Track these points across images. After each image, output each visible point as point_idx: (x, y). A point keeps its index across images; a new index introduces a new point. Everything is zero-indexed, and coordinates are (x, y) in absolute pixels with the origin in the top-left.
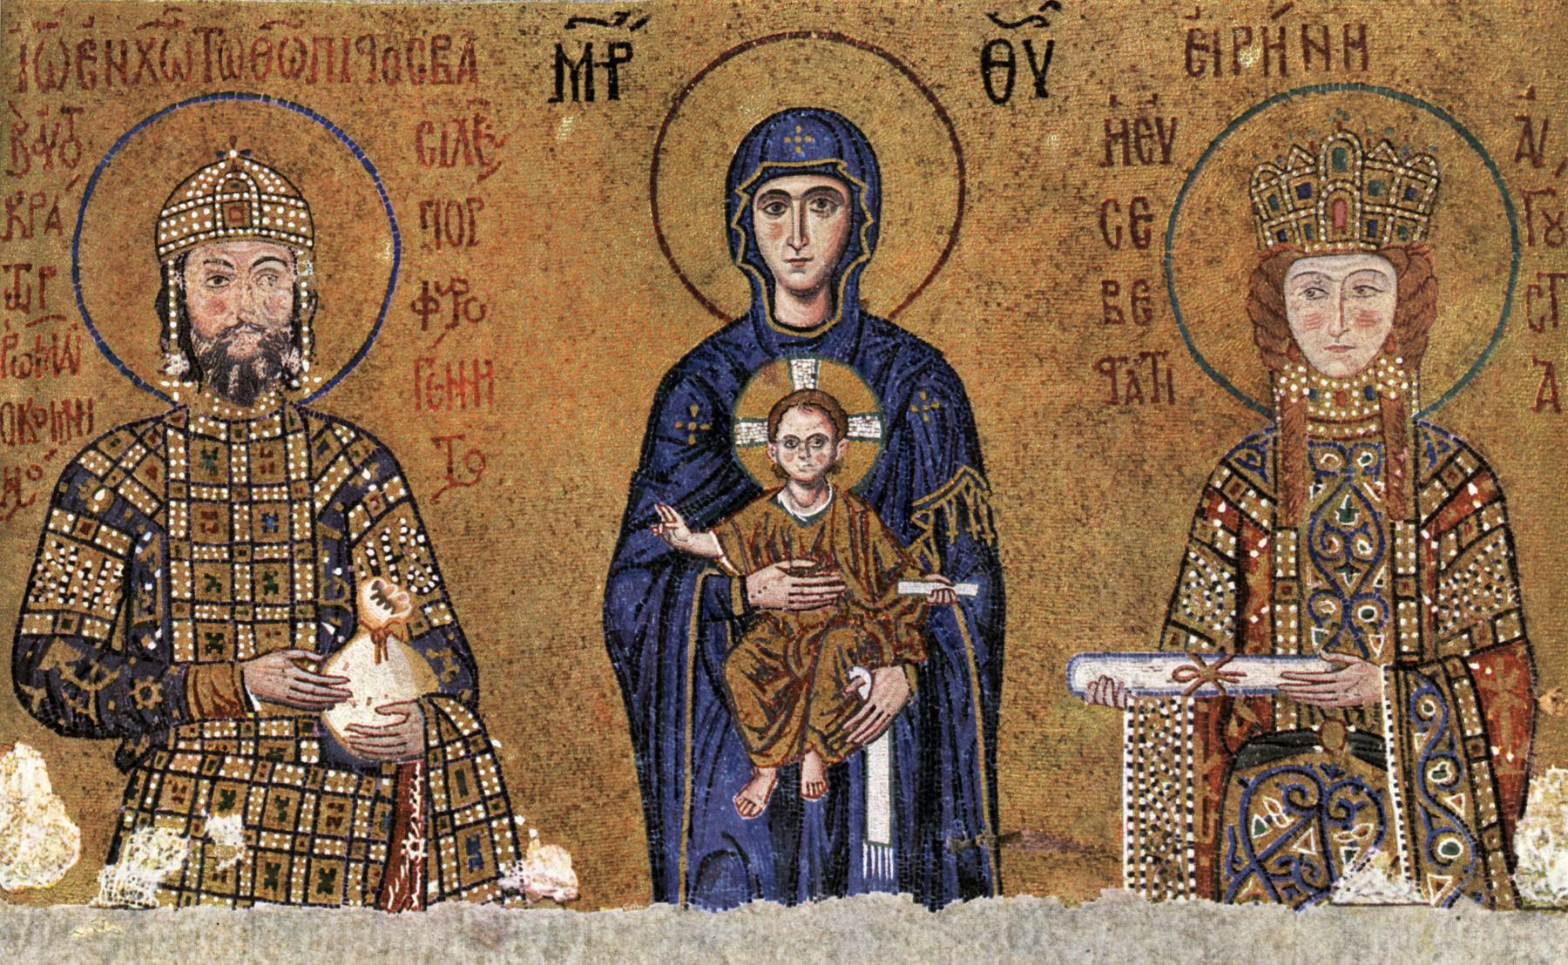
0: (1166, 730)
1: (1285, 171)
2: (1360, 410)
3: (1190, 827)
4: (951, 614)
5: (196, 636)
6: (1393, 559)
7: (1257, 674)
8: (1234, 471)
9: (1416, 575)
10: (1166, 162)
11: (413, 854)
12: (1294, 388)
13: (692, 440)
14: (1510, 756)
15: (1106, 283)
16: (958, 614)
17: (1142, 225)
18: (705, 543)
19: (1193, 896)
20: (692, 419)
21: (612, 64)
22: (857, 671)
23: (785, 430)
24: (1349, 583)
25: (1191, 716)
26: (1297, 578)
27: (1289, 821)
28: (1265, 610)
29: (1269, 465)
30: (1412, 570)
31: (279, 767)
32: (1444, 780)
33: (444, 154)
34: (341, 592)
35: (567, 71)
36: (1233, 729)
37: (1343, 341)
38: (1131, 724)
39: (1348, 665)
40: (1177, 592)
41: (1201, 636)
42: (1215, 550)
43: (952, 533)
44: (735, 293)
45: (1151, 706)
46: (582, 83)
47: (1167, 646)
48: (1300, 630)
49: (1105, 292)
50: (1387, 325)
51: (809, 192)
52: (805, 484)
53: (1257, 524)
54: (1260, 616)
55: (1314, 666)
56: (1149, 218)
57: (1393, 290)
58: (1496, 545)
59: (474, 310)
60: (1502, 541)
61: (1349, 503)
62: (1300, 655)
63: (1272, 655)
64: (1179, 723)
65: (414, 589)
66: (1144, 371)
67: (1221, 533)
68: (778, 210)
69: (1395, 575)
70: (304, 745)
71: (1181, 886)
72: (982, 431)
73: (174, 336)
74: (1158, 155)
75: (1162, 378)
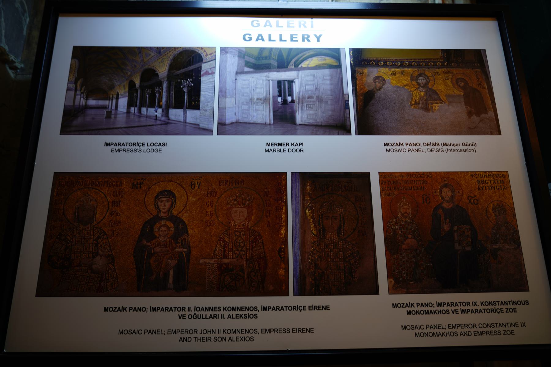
0: (213, 268)
1: (232, 197)
2: (242, 227)
3: (216, 281)
4: (183, 253)
5: (75, 255)
6: (246, 246)
7: (226, 261)
8: (224, 235)
9: (250, 248)
10: (216, 196)
11: (103, 285)
12: (232, 224)
13: (148, 231)
14: (263, 272)
15: (207, 211)
16: (184, 253)
17: (212, 204)
18: (149, 244)
19: (216, 291)
20: (147, 228)
21: (140, 184)
22: (169, 261)
23: (161, 229)
24: (240, 249)
25: (216, 266)
26: (232, 249)
27: (230, 280)
28: (228, 253)
29: (229, 234)
30: (249, 247)
31: (85, 273)
32: (253, 275)
33: (116, 194)
34: (96, 250)
35: (134, 185)
36: (223, 268)
37: (240, 218)
38: (208, 268)
39: (240, 260)
40: (215, 250)
41: (218, 256)
42: (221, 245)
43: (183, 243)
44: (155, 212)
45: (211, 265)
46: (136, 186)
47: (213, 257)
48: (232, 255)
49: (207, 212)
50: (245, 216)
51: (166, 200)
52: (163, 236)
53: (227, 242)
54: (227, 254)
55: (234, 260)
56: (213, 203)
57: (247, 212)
58: (261, 244)
59: (118, 214)
60: (262, 244)
61: (240, 239)
62: (233, 258)
63: (229, 258)
64: (215, 267)
65: (107, 250)
66: (212, 222)
67: (222, 243)
68: (162, 202)
69: (246, 248)
70: (89, 270)
71: (214, 289)
72: (188, 230)
73: (76, 218)
74: (215, 195)
75: (214, 223)
